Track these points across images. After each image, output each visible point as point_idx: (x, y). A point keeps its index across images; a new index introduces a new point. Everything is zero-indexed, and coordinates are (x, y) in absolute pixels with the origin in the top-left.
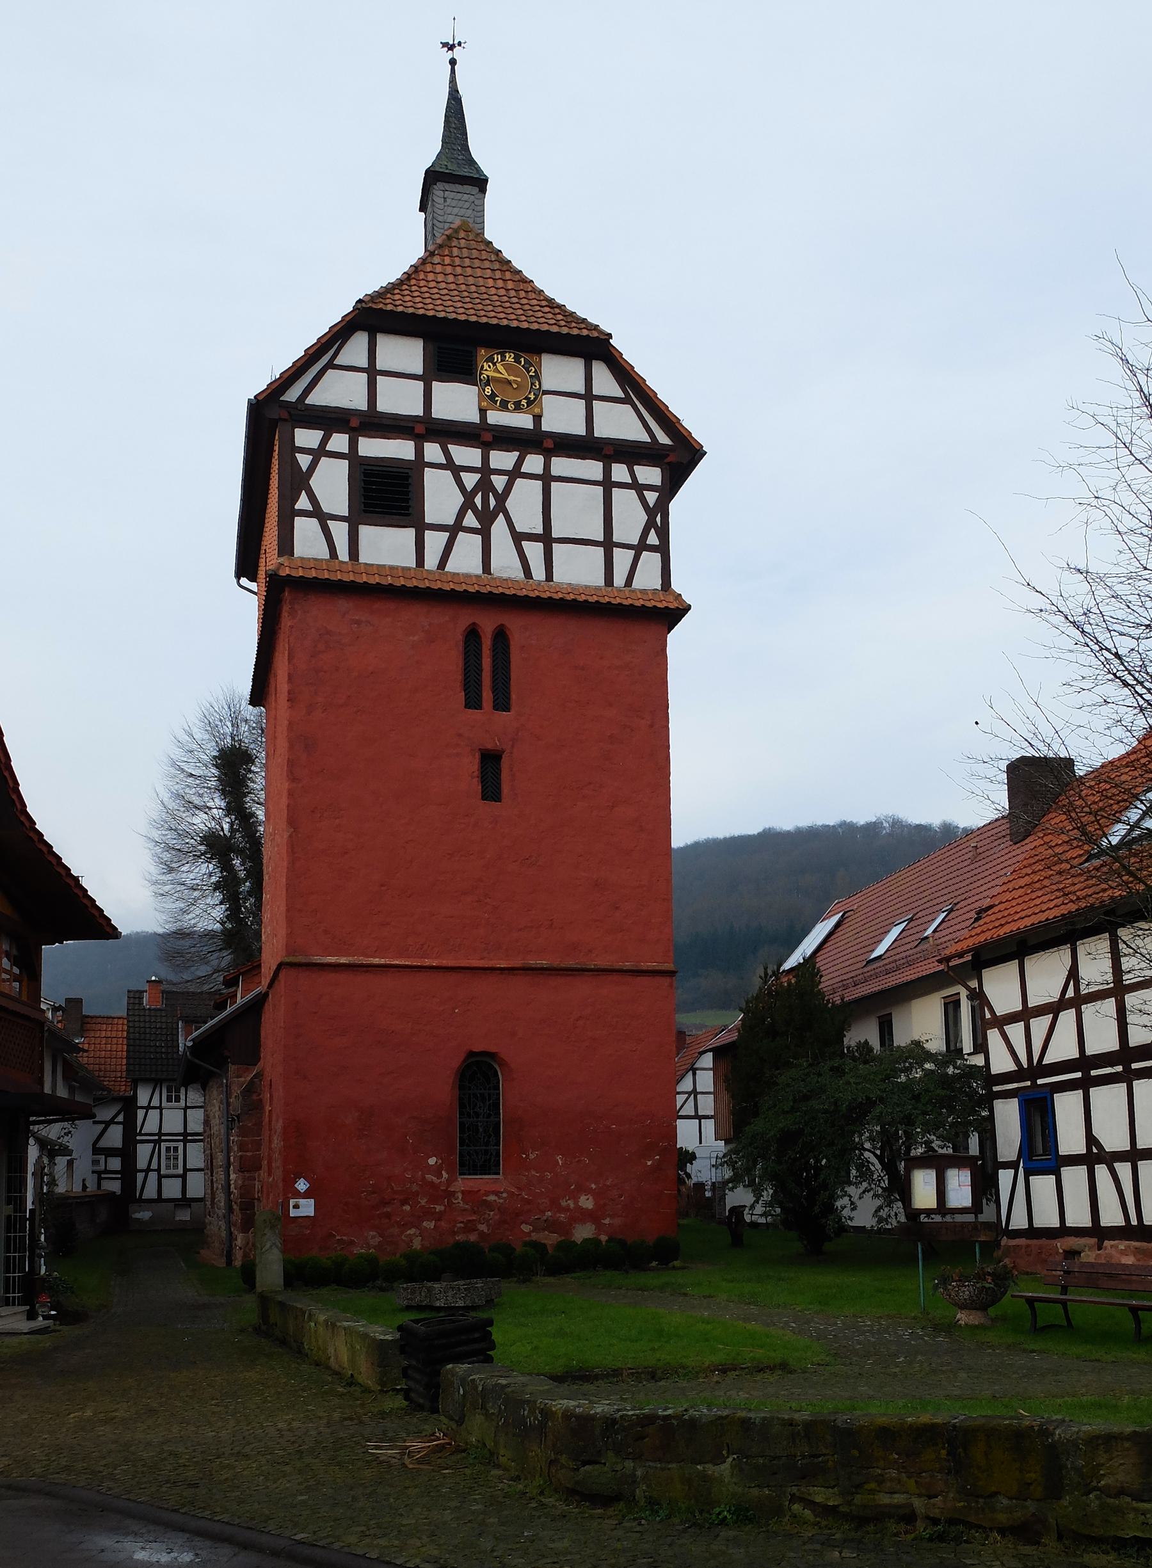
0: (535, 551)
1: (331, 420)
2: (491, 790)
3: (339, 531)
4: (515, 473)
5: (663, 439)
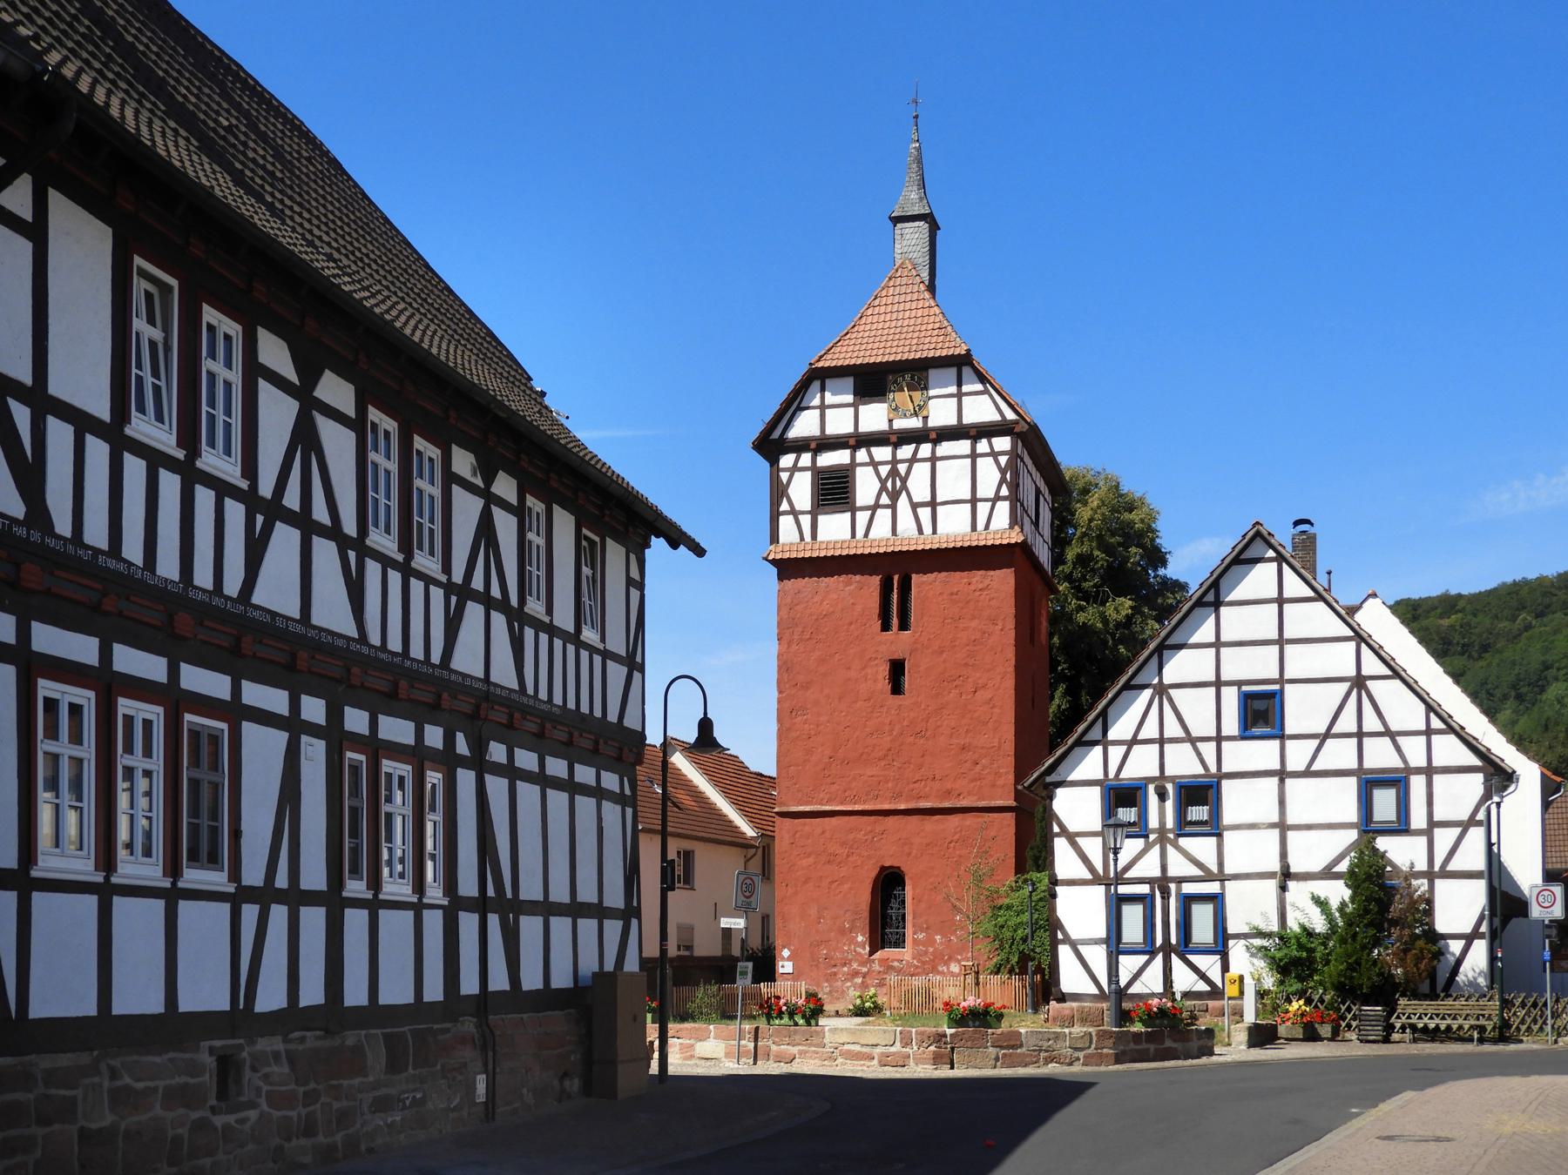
0: (925, 513)
1: (800, 446)
2: (897, 689)
3: (806, 521)
4: (913, 460)
5: (1010, 415)
